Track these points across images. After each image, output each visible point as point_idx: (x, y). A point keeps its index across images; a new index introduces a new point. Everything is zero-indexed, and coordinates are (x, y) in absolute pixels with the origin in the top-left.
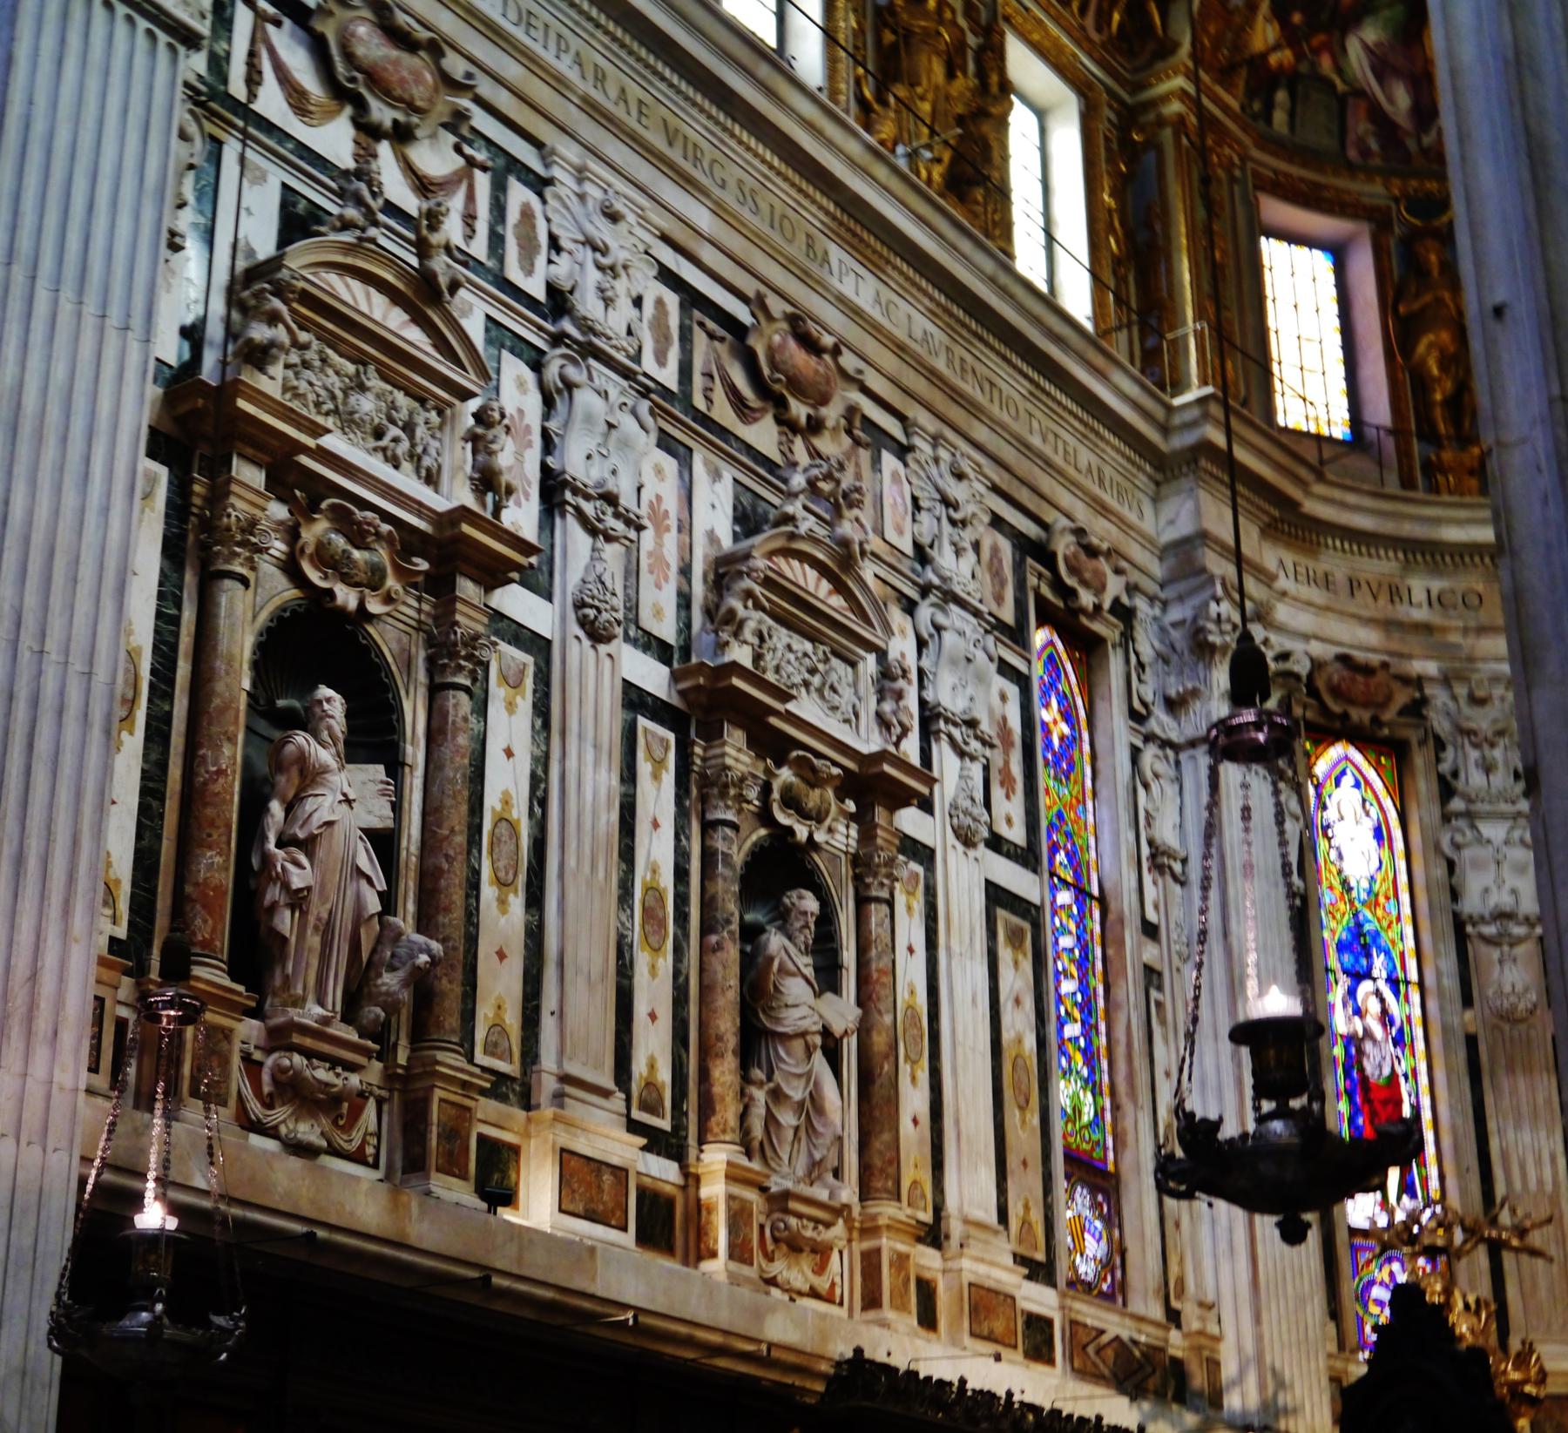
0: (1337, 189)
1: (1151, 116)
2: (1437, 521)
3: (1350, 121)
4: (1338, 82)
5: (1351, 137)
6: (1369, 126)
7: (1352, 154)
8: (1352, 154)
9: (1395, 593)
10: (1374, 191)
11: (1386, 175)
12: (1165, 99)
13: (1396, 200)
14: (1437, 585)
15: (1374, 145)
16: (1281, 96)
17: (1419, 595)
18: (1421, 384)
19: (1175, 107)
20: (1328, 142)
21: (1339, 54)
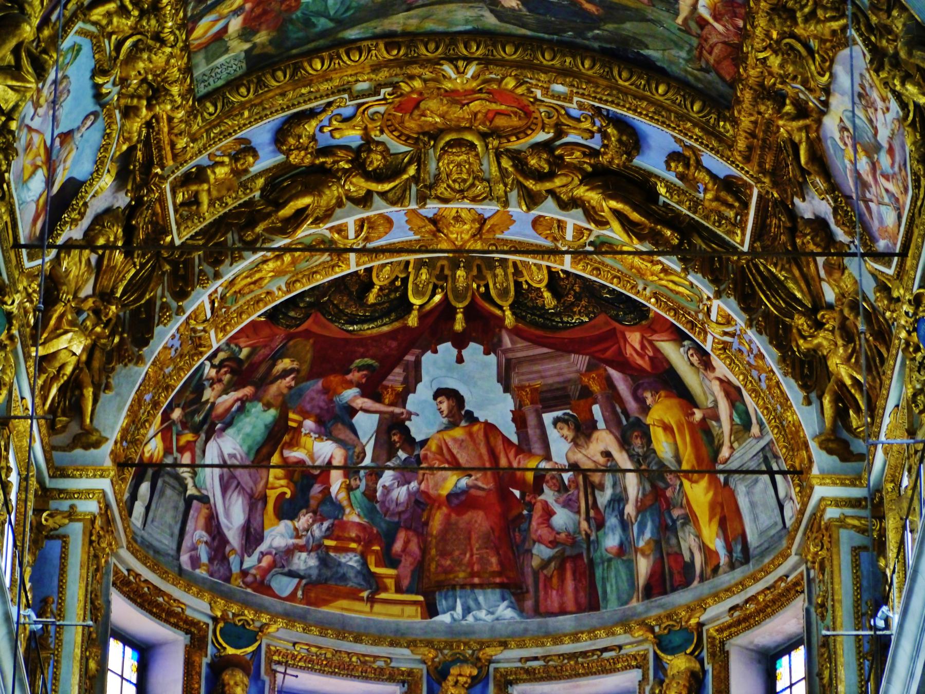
0: (170, 597)
1: (65, 505)
3: (190, 526)
4: (190, 482)
5: (187, 543)
6: (206, 537)
7: (185, 558)
8: (185, 558)
10: (198, 607)
11: (216, 592)
12: (85, 494)
13: (215, 620)
15: (204, 559)
16: (145, 487)
19: (90, 506)
20: (166, 542)
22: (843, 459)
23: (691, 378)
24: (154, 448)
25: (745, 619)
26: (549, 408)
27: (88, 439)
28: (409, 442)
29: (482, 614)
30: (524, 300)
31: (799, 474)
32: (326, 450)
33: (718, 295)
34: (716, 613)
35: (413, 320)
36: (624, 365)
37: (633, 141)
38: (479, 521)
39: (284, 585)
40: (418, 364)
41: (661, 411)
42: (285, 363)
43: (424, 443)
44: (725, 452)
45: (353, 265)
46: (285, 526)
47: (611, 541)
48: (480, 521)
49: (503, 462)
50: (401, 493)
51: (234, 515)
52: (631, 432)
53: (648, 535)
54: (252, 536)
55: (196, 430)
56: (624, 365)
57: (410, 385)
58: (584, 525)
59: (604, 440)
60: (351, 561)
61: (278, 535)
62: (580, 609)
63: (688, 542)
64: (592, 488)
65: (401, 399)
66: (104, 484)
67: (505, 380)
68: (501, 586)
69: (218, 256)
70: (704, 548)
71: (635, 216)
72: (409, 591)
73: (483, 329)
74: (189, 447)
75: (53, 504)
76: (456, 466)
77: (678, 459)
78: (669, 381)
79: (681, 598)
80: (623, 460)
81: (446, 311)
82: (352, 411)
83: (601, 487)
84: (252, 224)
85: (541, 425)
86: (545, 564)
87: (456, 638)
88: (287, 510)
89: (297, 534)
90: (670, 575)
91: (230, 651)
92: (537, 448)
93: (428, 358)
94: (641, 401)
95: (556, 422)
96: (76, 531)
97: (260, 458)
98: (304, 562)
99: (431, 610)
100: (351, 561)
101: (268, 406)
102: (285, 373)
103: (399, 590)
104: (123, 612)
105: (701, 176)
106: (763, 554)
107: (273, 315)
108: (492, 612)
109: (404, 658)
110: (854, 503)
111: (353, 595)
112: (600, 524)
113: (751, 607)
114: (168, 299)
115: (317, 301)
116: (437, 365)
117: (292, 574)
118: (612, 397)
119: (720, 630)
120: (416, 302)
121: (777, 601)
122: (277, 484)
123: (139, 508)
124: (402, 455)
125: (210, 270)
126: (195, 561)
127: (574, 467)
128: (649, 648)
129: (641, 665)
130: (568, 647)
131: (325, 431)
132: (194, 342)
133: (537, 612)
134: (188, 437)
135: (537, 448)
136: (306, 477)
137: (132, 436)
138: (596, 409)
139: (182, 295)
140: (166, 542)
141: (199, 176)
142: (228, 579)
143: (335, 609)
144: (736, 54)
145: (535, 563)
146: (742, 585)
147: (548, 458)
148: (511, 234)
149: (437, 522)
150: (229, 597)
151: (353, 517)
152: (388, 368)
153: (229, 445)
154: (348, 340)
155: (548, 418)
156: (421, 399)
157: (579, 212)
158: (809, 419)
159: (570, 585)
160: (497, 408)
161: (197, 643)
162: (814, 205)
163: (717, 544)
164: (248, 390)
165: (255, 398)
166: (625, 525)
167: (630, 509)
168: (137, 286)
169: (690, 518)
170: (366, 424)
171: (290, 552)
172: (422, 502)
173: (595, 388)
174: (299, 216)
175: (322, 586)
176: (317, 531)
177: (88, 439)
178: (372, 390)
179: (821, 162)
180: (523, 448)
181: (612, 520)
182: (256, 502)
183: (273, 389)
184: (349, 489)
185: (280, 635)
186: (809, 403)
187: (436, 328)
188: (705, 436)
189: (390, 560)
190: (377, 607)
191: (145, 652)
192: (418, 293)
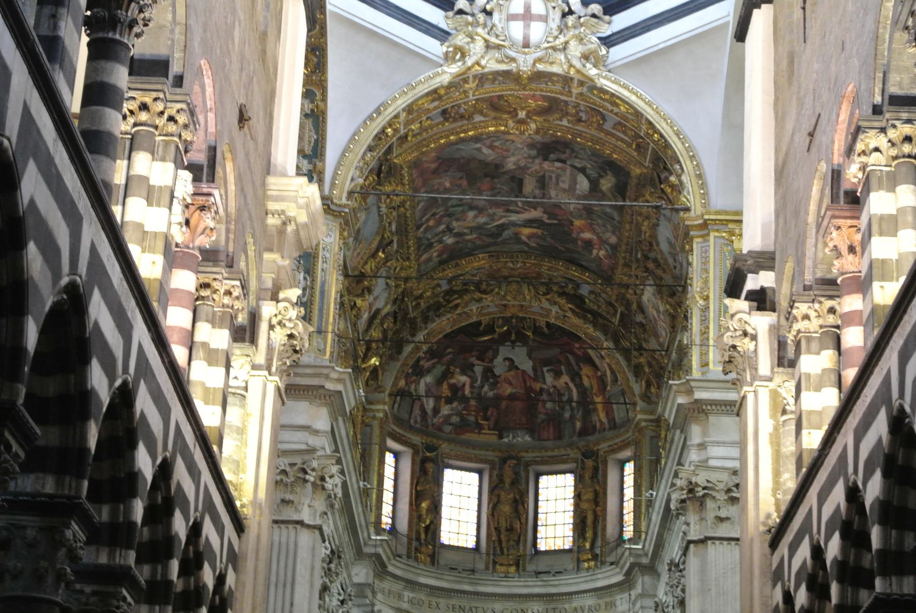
1: (371, 414)
2: (419, 575)
5: (413, 416)
7: (412, 421)
9: (400, 597)
10: (416, 439)
12: (378, 411)
14: (412, 595)
15: (419, 419)
16: (398, 398)
17: (406, 599)
18: (420, 517)
19: (381, 415)
20: (406, 416)
21: (417, 383)
22: (648, 403)
23: (597, 361)
24: (402, 383)
25: (614, 450)
26: (545, 366)
27: (379, 389)
28: (494, 376)
29: (519, 439)
30: (536, 330)
31: (634, 404)
32: (464, 379)
33: (606, 340)
34: (604, 446)
35: (496, 336)
36: (573, 353)
37: (577, 286)
38: (519, 405)
39: (447, 429)
40: (497, 350)
41: (586, 371)
42: (450, 350)
43: (499, 376)
44: (609, 388)
45: (475, 319)
46: (447, 407)
47: (567, 415)
48: (519, 405)
49: (528, 384)
50: (491, 394)
51: (430, 404)
52: (575, 376)
53: (580, 413)
54: (436, 411)
55: (417, 375)
56: (573, 353)
57: (495, 356)
58: (557, 408)
59: (565, 378)
60: (472, 419)
61: (445, 410)
62: (555, 439)
63: (595, 418)
64: (560, 395)
65: (491, 361)
66: (386, 407)
67: (530, 356)
68: (526, 429)
69: (426, 320)
70: (600, 421)
71: (577, 310)
72: (493, 430)
73: (522, 338)
74: (414, 381)
75: (368, 414)
76: (510, 384)
77: (592, 386)
78: (590, 361)
79: (590, 438)
80: (571, 385)
81: (508, 332)
82: (473, 365)
83: (564, 395)
84: (438, 309)
85: (543, 372)
86: (543, 421)
87: (510, 446)
88: (449, 401)
89: (452, 409)
90: (588, 430)
91: (428, 454)
92: (541, 380)
93: (501, 349)
94: (579, 366)
95: (548, 371)
96: (376, 424)
97: (439, 382)
98: (455, 419)
99: (501, 437)
100: (472, 419)
101: (442, 365)
102: (449, 354)
103: (489, 429)
104: (390, 443)
105: (601, 299)
106: (622, 426)
107: (446, 336)
108: (523, 438)
109: (490, 455)
110: (651, 421)
111: (472, 432)
112: (563, 409)
113: (615, 446)
114: (409, 337)
115: (461, 330)
116: (504, 351)
117: (450, 424)
118: (568, 364)
119: (605, 452)
120: (497, 330)
121: (624, 446)
122: (445, 390)
123: (396, 405)
124: (491, 380)
125: (423, 326)
126: (416, 422)
127: (554, 387)
128: (580, 456)
129: (576, 461)
130: (550, 453)
131: (463, 372)
132: (417, 349)
133: (540, 439)
134: (414, 378)
135: (541, 380)
136: (456, 390)
137: (395, 384)
138: (563, 368)
139: (413, 335)
140: (406, 416)
141: (421, 297)
142: (427, 427)
143: (467, 436)
144: (613, 268)
145: (539, 421)
146: (613, 438)
147: (545, 383)
148: (533, 310)
149: (504, 404)
150: (427, 434)
151: (473, 402)
152: (486, 352)
153: (429, 379)
154: (470, 343)
155: (545, 369)
156: (499, 359)
157: (557, 307)
158: (637, 388)
159: (551, 430)
160: (527, 365)
161: (415, 453)
162: (639, 318)
163: (604, 420)
164: (436, 360)
165: (438, 362)
166: (572, 409)
167: (574, 404)
168: (397, 332)
169: (595, 410)
170: (478, 370)
171: (450, 416)
172: (498, 398)
173: (562, 359)
174: (457, 306)
175: (463, 426)
176: (460, 408)
177: (379, 389)
178: (481, 358)
179: (641, 309)
180: (536, 379)
181: (568, 407)
182: (438, 398)
183: (445, 359)
184: (472, 393)
185: (445, 447)
186: (637, 382)
187: (504, 338)
188: (602, 381)
189: (486, 418)
190: (482, 436)
191: (397, 455)
192: (498, 327)
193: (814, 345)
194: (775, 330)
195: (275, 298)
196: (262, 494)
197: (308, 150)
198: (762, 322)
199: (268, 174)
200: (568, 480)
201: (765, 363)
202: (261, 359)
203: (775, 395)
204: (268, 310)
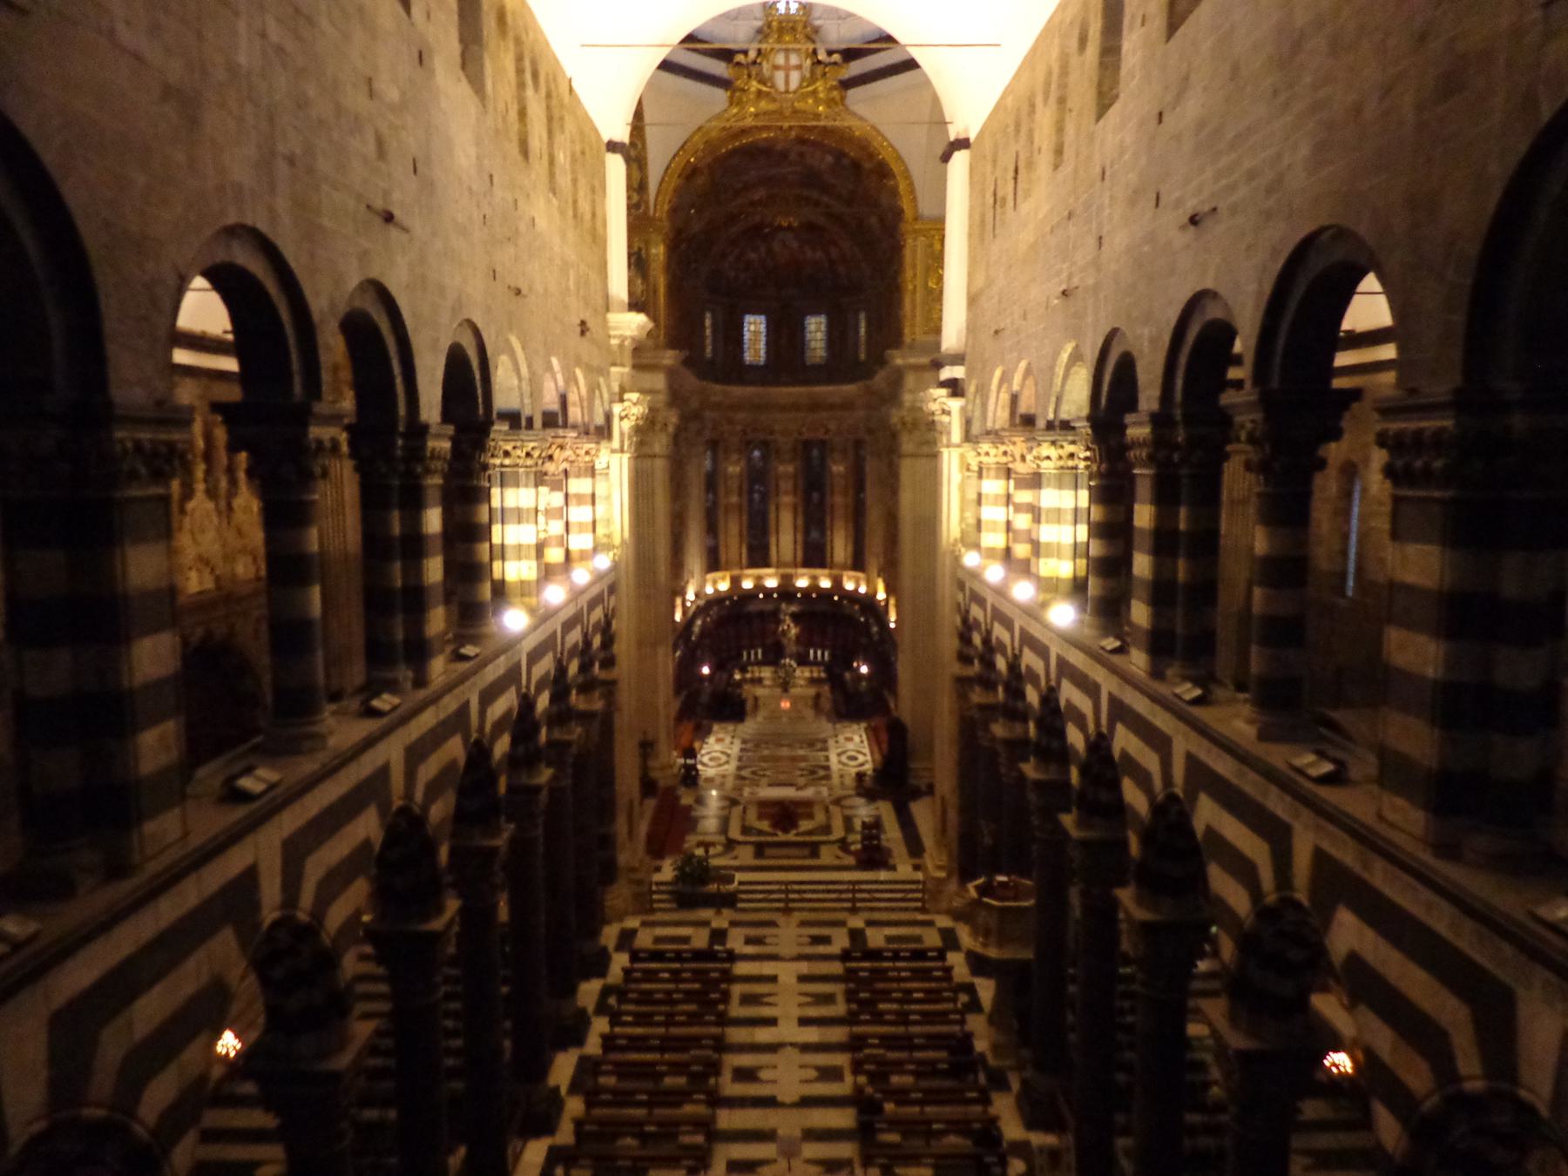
32: (753, 256)
59: (819, 255)
160: (795, 245)
191: (713, 312)
193: (992, 473)
194: (963, 409)
195: (622, 400)
196: (627, 534)
197: (635, 185)
198: (955, 405)
199: (608, 310)
200: (822, 319)
201: (956, 434)
202: (616, 444)
203: (962, 457)
204: (617, 409)
